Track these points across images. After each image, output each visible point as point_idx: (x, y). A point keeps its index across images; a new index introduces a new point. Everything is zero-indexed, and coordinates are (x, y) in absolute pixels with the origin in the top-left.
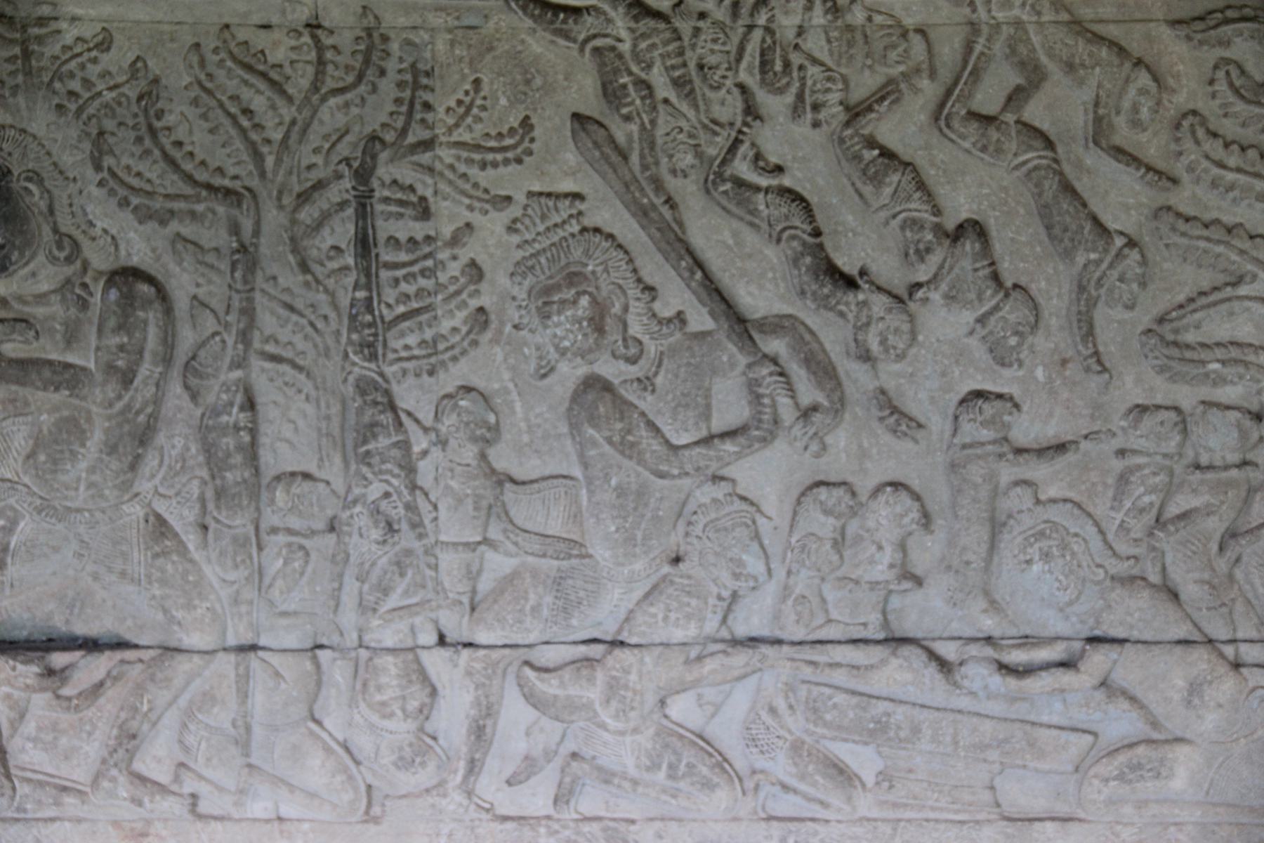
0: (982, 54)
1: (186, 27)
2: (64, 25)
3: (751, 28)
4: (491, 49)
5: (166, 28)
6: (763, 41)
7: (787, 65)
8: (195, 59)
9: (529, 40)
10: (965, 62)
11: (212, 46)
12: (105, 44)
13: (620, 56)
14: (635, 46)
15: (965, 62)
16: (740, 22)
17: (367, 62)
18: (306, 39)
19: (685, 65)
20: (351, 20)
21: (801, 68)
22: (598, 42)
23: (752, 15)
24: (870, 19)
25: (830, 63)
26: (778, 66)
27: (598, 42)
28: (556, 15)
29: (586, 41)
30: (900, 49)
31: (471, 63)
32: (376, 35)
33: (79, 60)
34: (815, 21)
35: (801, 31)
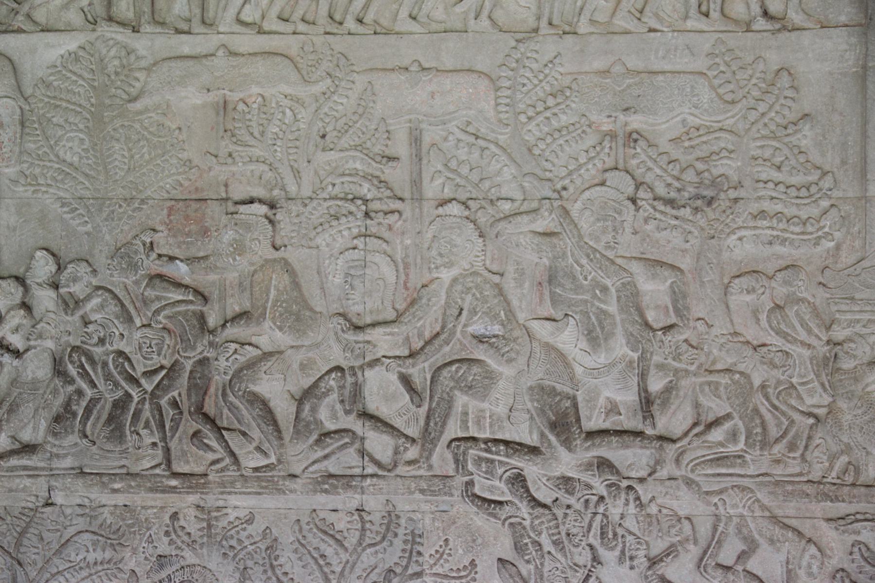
0: (723, 532)
1: (292, 511)
2: (229, 511)
3: (595, 514)
4: (454, 523)
5: (282, 511)
6: (602, 521)
7: (615, 534)
8: (297, 528)
9: (475, 518)
10: (713, 536)
11: (306, 521)
12: (250, 521)
13: (524, 528)
14: (532, 522)
15: (713, 536)
16: (590, 511)
17: (388, 529)
18: (356, 517)
19: (559, 533)
20: (380, 507)
21: (623, 536)
22: (512, 520)
23: (596, 507)
24: (660, 511)
25: (639, 535)
26: (610, 536)
27: (512, 520)
28: (489, 505)
29: (505, 520)
30: (677, 528)
31: (444, 530)
32: (393, 515)
33: (236, 529)
34: (630, 512)
35: (622, 517)
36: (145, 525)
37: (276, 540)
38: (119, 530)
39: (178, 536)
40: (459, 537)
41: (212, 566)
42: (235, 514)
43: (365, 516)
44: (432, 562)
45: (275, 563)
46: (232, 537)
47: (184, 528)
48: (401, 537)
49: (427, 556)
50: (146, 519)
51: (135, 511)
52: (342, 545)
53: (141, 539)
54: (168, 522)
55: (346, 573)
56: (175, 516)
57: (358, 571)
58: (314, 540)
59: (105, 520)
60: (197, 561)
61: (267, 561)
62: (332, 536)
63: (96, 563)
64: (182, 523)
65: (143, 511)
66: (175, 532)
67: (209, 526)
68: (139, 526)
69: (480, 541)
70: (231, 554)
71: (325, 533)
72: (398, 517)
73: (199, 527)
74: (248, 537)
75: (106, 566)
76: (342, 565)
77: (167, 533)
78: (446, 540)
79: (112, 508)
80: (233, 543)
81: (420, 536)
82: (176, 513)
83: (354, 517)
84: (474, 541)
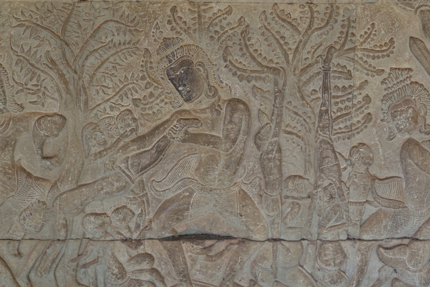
1: (260, 4)
2: (214, 5)
4: (379, 11)
8: (263, 17)
9: (395, 7)
11: (270, 12)
12: (229, 12)
17: (330, 17)
18: (307, 8)
22: (423, 8)
27: (423, 8)
29: (418, 8)
31: (371, 17)
32: (334, 6)
33: (220, 18)
36: (153, 16)
37: (248, 26)
38: (134, 19)
39: (177, 24)
40: (382, 21)
41: (203, 45)
42: (218, 8)
43: (313, 8)
44: (362, 40)
45: (248, 43)
46: (216, 25)
47: (181, 18)
48: (340, 23)
49: (358, 36)
50: (154, 12)
51: (145, 5)
52: (297, 30)
53: (151, 26)
54: (170, 13)
55: (300, 49)
56: (174, 10)
57: (308, 47)
58: (275, 27)
59: (124, 12)
60: (192, 43)
61: (242, 41)
62: (290, 23)
63: (120, 44)
64: (180, 14)
65: (151, 5)
66: (175, 21)
67: (200, 16)
68: (149, 17)
69: (397, 24)
70: (217, 37)
71: (284, 20)
72: (338, 8)
73: (192, 17)
74: (228, 24)
75: (127, 46)
76: (296, 44)
77: (169, 22)
78: (373, 24)
79: (128, 3)
80: (218, 28)
81: (354, 22)
82: (175, 7)
83: (305, 9)
84: (393, 24)
